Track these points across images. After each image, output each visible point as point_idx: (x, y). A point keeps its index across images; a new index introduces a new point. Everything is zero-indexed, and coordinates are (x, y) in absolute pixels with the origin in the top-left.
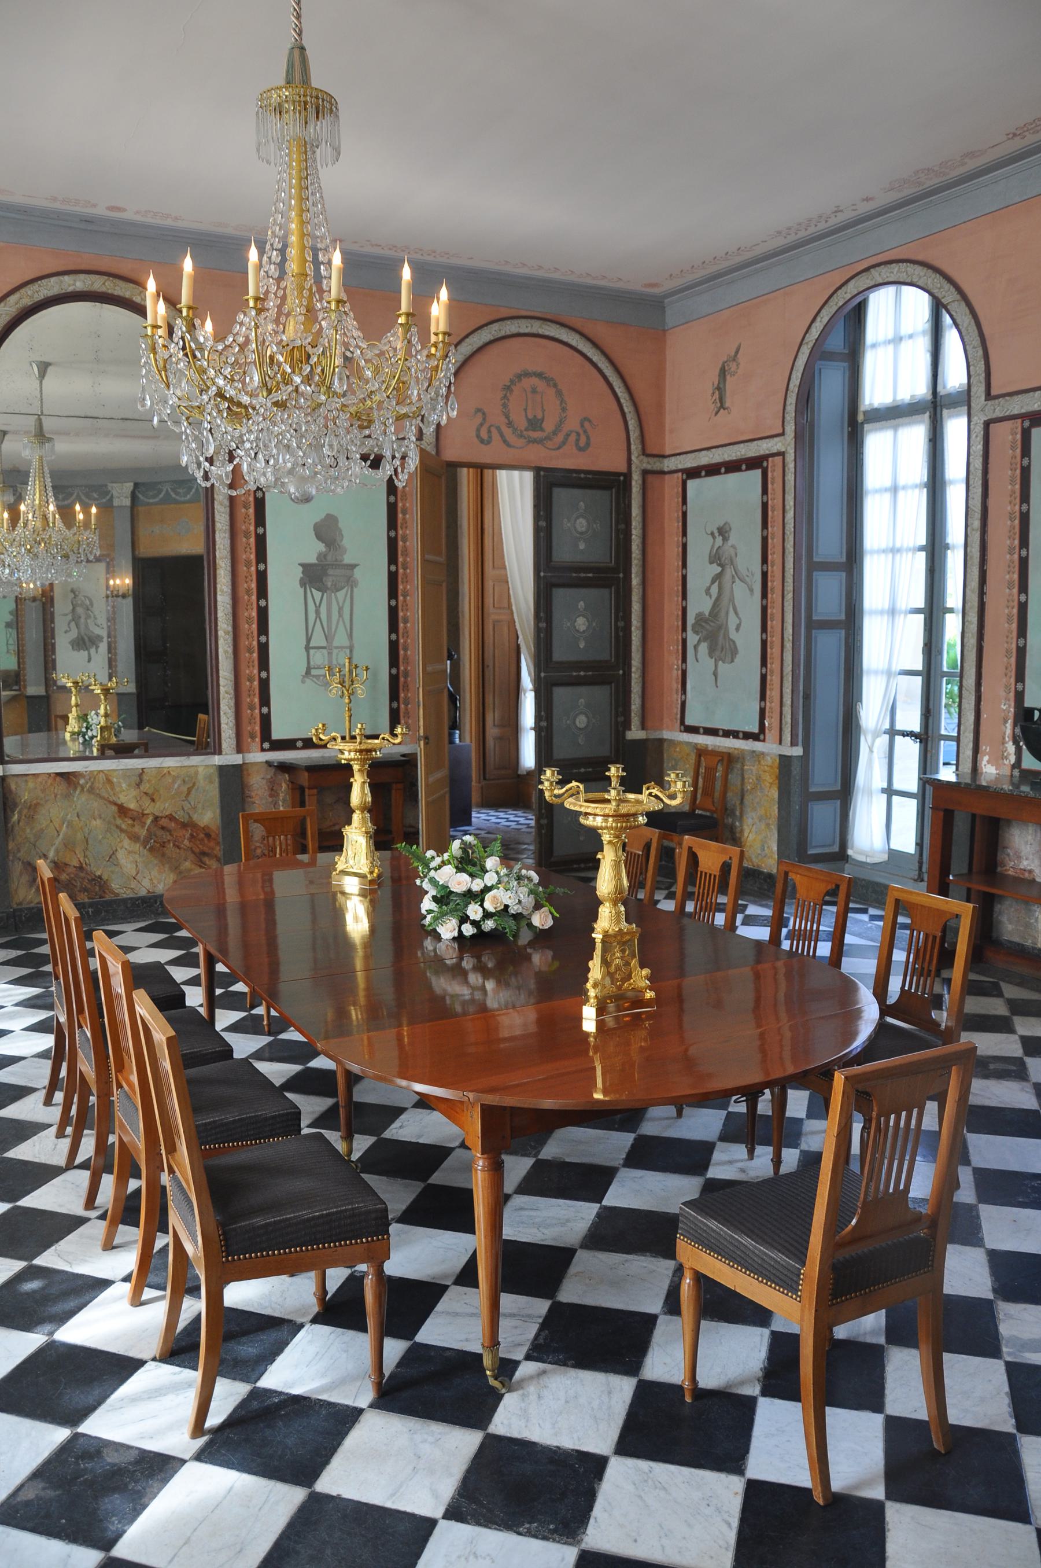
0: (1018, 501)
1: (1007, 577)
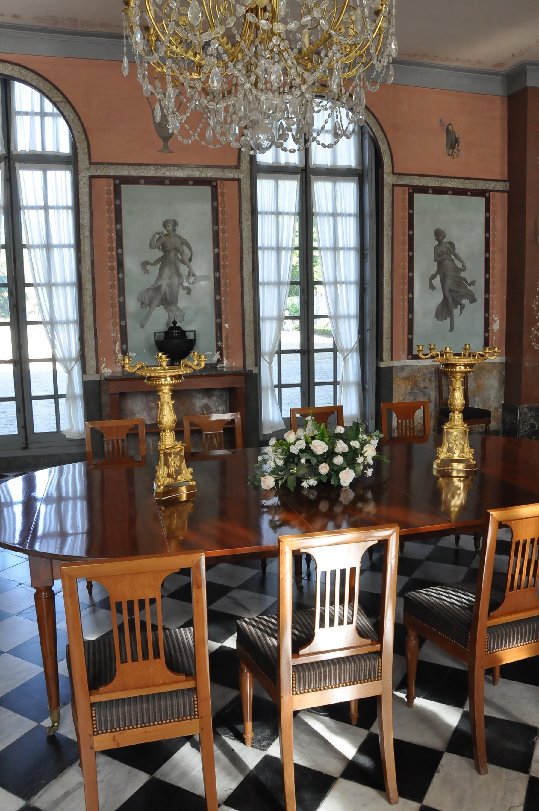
0: (114, 222)
1: (109, 264)
